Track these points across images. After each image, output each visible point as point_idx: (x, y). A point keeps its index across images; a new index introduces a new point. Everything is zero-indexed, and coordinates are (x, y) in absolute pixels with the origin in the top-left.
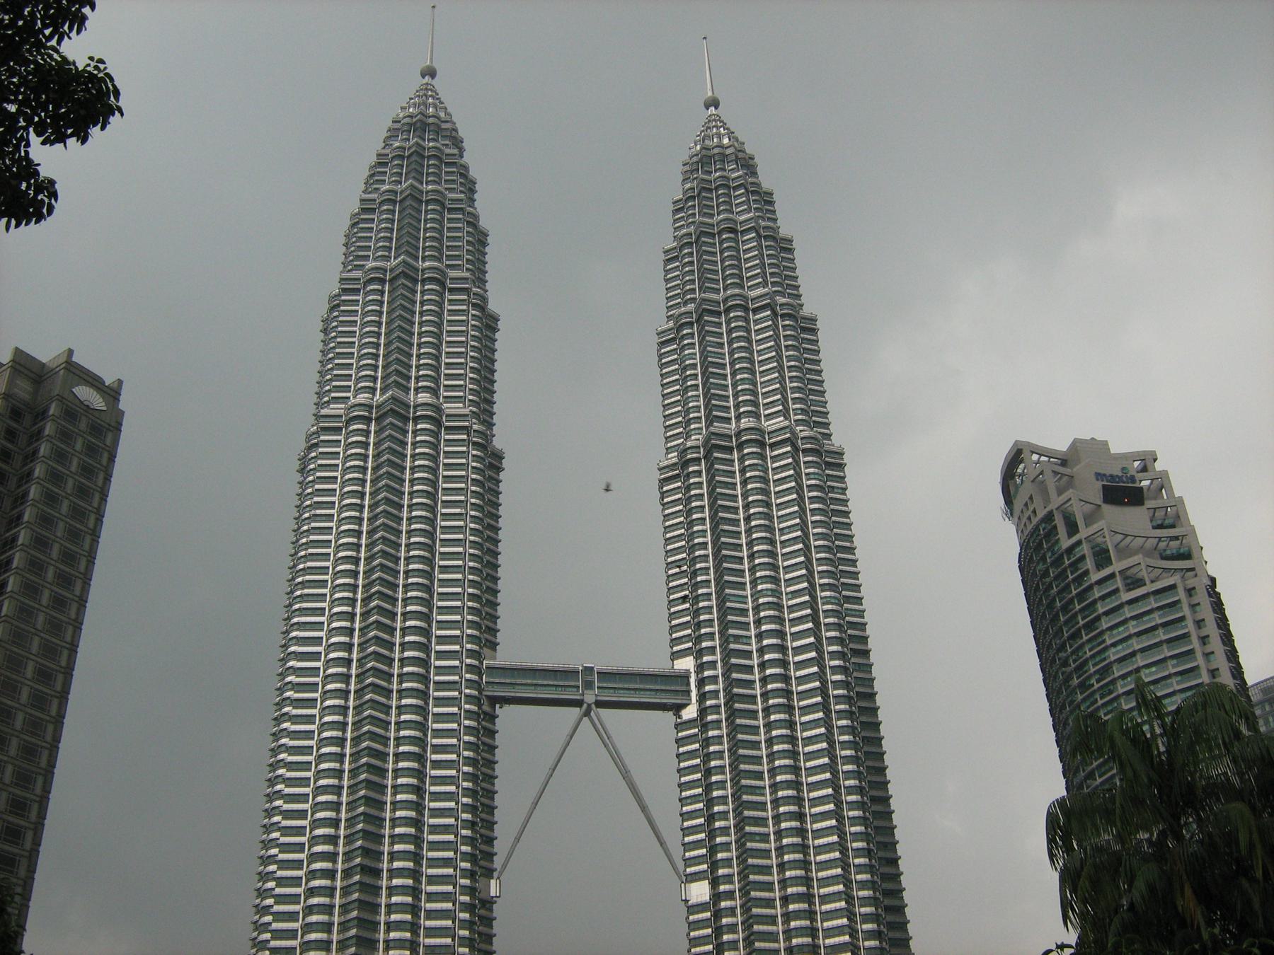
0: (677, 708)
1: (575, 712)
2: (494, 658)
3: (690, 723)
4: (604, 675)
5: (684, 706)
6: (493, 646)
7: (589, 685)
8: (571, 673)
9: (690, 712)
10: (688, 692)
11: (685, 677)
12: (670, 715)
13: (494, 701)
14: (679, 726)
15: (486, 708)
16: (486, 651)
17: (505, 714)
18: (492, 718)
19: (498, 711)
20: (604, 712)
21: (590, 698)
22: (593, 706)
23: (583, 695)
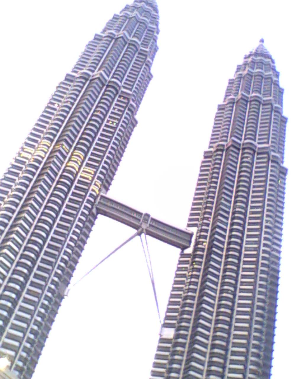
0: (184, 248)
1: (134, 231)
2: (106, 194)
3: (188, 255)
4: (153, 219)
6: (107, 189)
7: (146, 221)
8: (140, 214)
9: (189, 251)
10: (190, 242)
11: (191, 235)
13: (99, 211)
16: (104, 190)
19: (100, 216)
20: (148, 237)
21: (144, 226)
22: (144, 231)
23: (141, 224)
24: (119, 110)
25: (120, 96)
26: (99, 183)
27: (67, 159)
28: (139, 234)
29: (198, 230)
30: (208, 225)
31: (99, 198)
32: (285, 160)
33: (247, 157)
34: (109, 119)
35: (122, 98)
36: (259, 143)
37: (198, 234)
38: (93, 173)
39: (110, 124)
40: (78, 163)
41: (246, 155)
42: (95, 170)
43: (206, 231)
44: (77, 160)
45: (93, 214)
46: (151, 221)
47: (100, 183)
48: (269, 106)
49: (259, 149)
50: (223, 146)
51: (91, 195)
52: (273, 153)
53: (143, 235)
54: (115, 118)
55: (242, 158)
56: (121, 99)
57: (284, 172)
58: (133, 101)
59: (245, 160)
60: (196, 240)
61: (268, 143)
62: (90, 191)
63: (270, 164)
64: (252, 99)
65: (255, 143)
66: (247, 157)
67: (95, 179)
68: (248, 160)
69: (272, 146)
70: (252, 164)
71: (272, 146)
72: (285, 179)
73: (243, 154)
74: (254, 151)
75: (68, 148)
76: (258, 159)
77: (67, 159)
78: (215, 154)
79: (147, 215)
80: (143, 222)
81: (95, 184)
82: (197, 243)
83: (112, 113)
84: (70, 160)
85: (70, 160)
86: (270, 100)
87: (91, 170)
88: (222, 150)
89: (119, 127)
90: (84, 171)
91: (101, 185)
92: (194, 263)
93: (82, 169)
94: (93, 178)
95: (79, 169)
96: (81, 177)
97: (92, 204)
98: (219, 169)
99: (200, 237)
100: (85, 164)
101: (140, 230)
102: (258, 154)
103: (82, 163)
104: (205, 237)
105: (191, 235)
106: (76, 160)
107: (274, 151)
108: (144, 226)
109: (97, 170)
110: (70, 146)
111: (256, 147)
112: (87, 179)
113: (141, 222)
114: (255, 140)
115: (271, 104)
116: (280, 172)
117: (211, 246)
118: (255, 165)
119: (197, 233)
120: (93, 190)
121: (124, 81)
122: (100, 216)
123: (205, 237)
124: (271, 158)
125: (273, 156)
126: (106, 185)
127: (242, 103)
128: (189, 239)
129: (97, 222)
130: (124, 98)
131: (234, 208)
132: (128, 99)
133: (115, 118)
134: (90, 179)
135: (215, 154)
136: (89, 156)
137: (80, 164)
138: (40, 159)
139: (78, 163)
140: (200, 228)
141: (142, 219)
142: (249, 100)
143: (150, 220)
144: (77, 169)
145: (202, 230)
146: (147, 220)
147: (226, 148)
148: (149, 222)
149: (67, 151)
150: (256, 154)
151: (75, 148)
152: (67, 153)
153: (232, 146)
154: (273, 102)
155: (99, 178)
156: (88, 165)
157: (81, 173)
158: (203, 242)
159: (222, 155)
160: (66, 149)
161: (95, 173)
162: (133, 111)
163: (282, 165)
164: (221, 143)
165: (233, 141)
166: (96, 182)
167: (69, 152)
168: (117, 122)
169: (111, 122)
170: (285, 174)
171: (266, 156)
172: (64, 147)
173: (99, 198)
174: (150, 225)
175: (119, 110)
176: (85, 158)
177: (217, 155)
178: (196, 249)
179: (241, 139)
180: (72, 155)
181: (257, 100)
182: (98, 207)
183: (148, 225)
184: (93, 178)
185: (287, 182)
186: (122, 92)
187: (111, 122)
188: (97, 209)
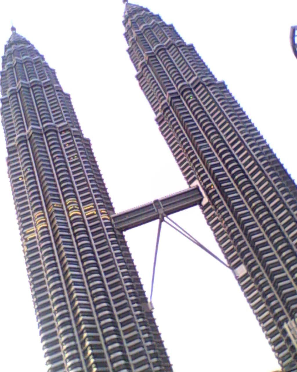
0: (199, 202)
1: (157, 221)
2: (114, 213)
3: (207, 205)
4: (163, 201)
5: (201, 200)
7: (158, 207)
9: (205, 201)
10: (201, 194)
11: (197, 188)
12: (197, 207)
14: (203, 208)
15: (118, 233)
16: (111, 212)
17: (127, 234)
18: (123, 237)
19: (124, 233)
20: (169, 216)
21: (161, 211)
22: (164, 215)
24: (69, 144)
25: (61, 133)
26: (103, 210)
27: (66, 212)
28: (162, 220)
29: (199, 181)
30: (203, 171)
31: (113, 221)
32: (216, 76)
33: (189, 98)
34: (69, 156)
35: (63, 133)
36: (189, 80)
37: (202, 184)
38: (93, 207)
39: (72, 160)
40: (76, 209)
41: (187, 97)
42: (92, 204)
43: (206, 176)
44: (74, 206)
45: (119, 236)
46: (162, 204)
47: (104, 209)
48: (173, 46)
49: (192, 84)
50: (166, 104)
51: (106, 224)
52: (204, 79)
53: (165, 219)
54: (72, 153)
55: (187, 102)
56: (64, 134)
57: (223, 86)
58: (73, 127)
59: (189, 101)
60: (204, 189)
61: (194, 75)
62: (103, 222)
63: (209, 88)
64: (157, 51)
65: (186, 83)
66: (189, 98)
67: (99, 210)
68: (192, 99)
69: (199, 74)
70: (196, 100)
71: (199, 74)
72: (228, 91)
73: (184, 98)
74: (191, 89)
75: (59, 203)
76: (197, 92)
77: (66, 212)
78: (165, 115)
79: (156, 201)
80: (157, 209)
81: (102, 214)
82: (207, 191)
83: (66, 150)
84: (68, 211)
85: (68, 211)
86: (170, 41)
87: (91, 206)
88: (168, 108)
89: (81, 156)
90: (86, 211)
91: (106, 211)
92: (217, 207)
93: (83, 210)
94: (97, 211)
95: (81, 211)
96: (88, 216)
97: (112, 229)
98: (177, 124)
99: (205, 184)
100: (81, 205)
101: (160, 217)
102: (195, 88)
103: (79, 206)
104: (209, 182)
105: (197, 188)
106: (73, 207)
107: (202, 77)
108: (161, 211)
109: (94, 202)
110: (60, 201)
111: (188, 85)
112: (93, 214)
113: (156, 211)
114: (184, 81)
115: (173, 44)
116: (221, 88)
117: (219, 184)
118: (199, 99)
119: (201, 184)
120: (104, 219)
121: (53, 118)
122: (124, 233)
123: (209, 182)
124: (206, 84)
125: (206, 81)
126: (108, 206)
127: (152, 61)
128: (198, 193)
129: (127, 239)
130: (65, 131)
131: (212, 143)
132: (69, 130)
133: (72, 153)
134: (95, 212)
135: (165, 115)
136: (79, 196)
137: (78, 208)
138: (45, 230)
139: (76, 209)
140: (200, 179)
141: (155, 208)
142: (155, 53)
143: (160, 203)
144: (80, 213)
145: (202, 179)
146: (160, 205)
147: (169, 104)
148: (161, 205)
149: (61, 206)
150: (193, 90)
151: (65, 199)
152: (62, 207)
153: (172, 98)
154: (173, 41)
155: (100, 207)
156: (84, 204)
157: (85, 214)
158: (210, 187)
159: (171, 112)
160: (58, 206)
161: (95, 205)
162: (79, 135)
163: (217, 82)
164: (162, 103)
165: (170, 94)
166: (100, 211)
167: (62, 205)
168: (76, 154)
169: (72, 158)
170: (225, 87)
171: (201, 85)
172: (55, 205)
173: (113, 221)
174: (164, 207)
175: (69, 144)
176: (77, 200)
177: (167, 114)
178: (209, 196)
179: (174, 88)
180: (66, 206)
181: (160, 49)
182: (118, 227)
183: (163, 208)
184: (97, 211)
185: (231, 91)
186: (60, 128)
187: (72, 158)
188: (118, 229)
